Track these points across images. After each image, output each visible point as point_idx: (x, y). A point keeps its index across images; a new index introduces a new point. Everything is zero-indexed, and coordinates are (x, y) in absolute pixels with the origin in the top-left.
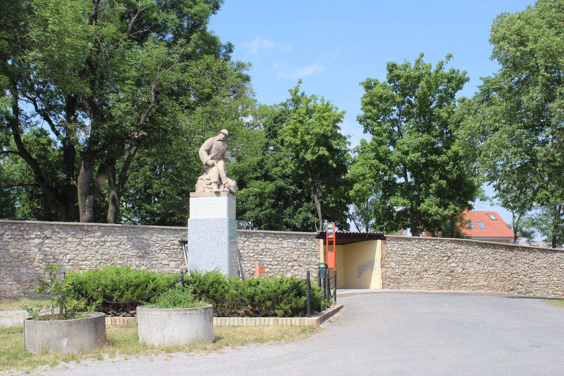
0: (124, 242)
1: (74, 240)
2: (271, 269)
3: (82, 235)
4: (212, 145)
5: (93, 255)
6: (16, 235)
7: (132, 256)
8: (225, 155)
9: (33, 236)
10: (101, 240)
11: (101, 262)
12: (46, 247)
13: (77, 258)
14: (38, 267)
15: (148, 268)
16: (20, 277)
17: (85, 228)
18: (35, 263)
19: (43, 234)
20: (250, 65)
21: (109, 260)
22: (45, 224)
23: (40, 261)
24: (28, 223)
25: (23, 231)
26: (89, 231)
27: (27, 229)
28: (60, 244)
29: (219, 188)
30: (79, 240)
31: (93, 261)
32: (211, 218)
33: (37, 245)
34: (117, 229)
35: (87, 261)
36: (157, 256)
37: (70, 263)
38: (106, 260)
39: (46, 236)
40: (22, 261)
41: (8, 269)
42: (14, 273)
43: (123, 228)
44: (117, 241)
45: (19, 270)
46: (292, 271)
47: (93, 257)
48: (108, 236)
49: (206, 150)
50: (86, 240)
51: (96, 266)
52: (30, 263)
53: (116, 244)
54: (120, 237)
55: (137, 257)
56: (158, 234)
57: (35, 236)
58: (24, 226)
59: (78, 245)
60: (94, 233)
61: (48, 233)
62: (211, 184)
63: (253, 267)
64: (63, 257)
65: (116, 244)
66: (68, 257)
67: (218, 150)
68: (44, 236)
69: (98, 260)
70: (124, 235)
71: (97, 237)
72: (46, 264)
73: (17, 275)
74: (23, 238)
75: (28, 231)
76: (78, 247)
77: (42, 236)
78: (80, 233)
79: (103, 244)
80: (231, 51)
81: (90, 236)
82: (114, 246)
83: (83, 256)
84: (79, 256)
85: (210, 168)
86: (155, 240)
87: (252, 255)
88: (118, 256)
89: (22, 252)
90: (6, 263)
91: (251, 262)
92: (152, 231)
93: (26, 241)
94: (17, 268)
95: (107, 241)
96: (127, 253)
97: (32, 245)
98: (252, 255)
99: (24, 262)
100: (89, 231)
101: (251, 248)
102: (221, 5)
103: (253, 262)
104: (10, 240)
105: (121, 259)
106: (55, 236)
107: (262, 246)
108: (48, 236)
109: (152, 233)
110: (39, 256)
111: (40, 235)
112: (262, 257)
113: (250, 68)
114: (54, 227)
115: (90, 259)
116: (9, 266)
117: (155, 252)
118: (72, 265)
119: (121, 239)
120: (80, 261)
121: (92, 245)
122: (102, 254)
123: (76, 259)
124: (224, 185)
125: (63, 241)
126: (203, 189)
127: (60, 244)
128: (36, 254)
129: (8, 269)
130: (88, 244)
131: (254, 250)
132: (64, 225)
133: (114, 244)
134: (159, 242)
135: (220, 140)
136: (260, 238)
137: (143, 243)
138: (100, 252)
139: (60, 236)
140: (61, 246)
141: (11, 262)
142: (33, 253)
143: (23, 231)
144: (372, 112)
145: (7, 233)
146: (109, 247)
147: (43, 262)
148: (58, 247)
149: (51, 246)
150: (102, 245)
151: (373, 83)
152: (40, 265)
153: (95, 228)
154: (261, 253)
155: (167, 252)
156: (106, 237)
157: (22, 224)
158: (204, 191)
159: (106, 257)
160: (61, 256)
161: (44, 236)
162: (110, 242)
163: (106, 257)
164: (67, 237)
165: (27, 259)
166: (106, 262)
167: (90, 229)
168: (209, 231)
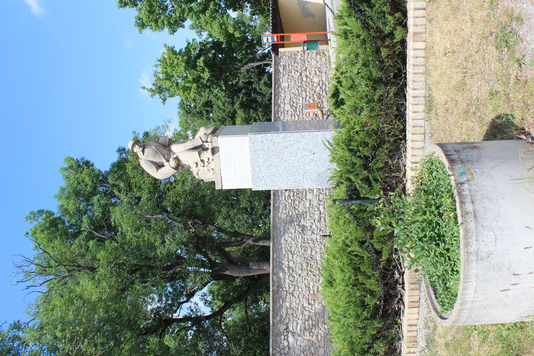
0: (289, 248)
1: (288, 299)
2: (310, 98)
3: (283, 292)
4: (150, 161)
5: (303, 279)
8: (164, 143)
10: (287, 271)
11: (310, 271)
12: (296, 328)
13: (307, 296)
14: (317, 336)
15: (315, 221)
17: (276, 288)
18: (313, 340)
19: (284, 333)
20: (134, 132)
21: (308, 262)
22: (273, 331)
23: (312, 334)
26: (279, 284)
27: (279, 350)
28: (293, 314)
29: (207, 149)
30: (288, 294)
31: (309, 279)
32: (249, 158)
33: (295, 338)
34: (275, 256)
35: (309, 285)
36: (301, 213)
37: (313, 303)
39: (285, 329)
40: (312, 354)
43: (275, 249)
44: (288, 255)
46: (311, 77)
47: (305, 279)
48: (283, 264)
49: (157, 170)
50: (288, 287)
51: (315, 275)
52: (314, 344)
54: (284, 252)
55: (303, 233)
56: (279, 212)
57: (285, 341)
58: (276, 354)
59: (293, 296)
60: (280, 279)
61: (282, 328)
62: (202, 161)
63: (309, 115)
64: (306, 310)
65: (291, 256)
66: (306, 305)
67: (156, 153)
68: (285, 332)
69: (308, 274)
70: (282, 247)
72: (314, 328)
77: (285, 334)
78: (281, 294)
79: (291, 269)
80: (124, 149)
81: (284, 282)
82: (293, 257)
83: (304, 290)
84: (305, 293)
85: (181, 163)
86: (285, 216)
87: (297, 117)
88: (303, 253)
89: (302, 354)
91: (304, 117)
92: (277, 219)
93: (292, 351)
95: (288, 265)
98: (297, 117)
99: (313, 351)
100: (279, 284)
101: (289, 118)
102: (86, 159)
103: (304, 115)
105: (306, 249)
106: (285, 320)
107: (287, 108)
108: (285, 328)
109: (278, 219)
110: (307, 336)
111: (285, 336)
112: (298, 107)
113: (137, 132)
114: (275, 322)
117: (297, 214)
118: (314, 300)
119: (286, 251)
120: (310, 293)
121: (293, 280)
122: (302, 269)
123: (308, 297)
124: (203, 142)
125: (290, 312)
126: (211, 171)
127: (293, 314)
128: (304, 339)
130: (292, 285)
131: (292, 115)
132: (273, 311)
133: (290, 258)
134: (287, 211)
135: (143, 151)
136: (280, 110)
138: (300, 272)
139: (284, 315)
140: (295, 313)
142: (303, 342)
143: (281, 354)
144: (164, 20)
146: (294, 263)
147: (312, 332)
148: (296, 316)
149: (295, 324)
150: (293, 271)
151: (138, 21)
152: (315, 334)
153: (275, 279)
154: (294, 107)
155: (297, 203)
156: (284, 266)
158: (213, 169)
159: (304, 265)
160: (305, 312)
161: (285, 332)
162: (289, 262)
163: (304, 265)
166: (309, 265)
167: (277, 284)
168: (269, 160)
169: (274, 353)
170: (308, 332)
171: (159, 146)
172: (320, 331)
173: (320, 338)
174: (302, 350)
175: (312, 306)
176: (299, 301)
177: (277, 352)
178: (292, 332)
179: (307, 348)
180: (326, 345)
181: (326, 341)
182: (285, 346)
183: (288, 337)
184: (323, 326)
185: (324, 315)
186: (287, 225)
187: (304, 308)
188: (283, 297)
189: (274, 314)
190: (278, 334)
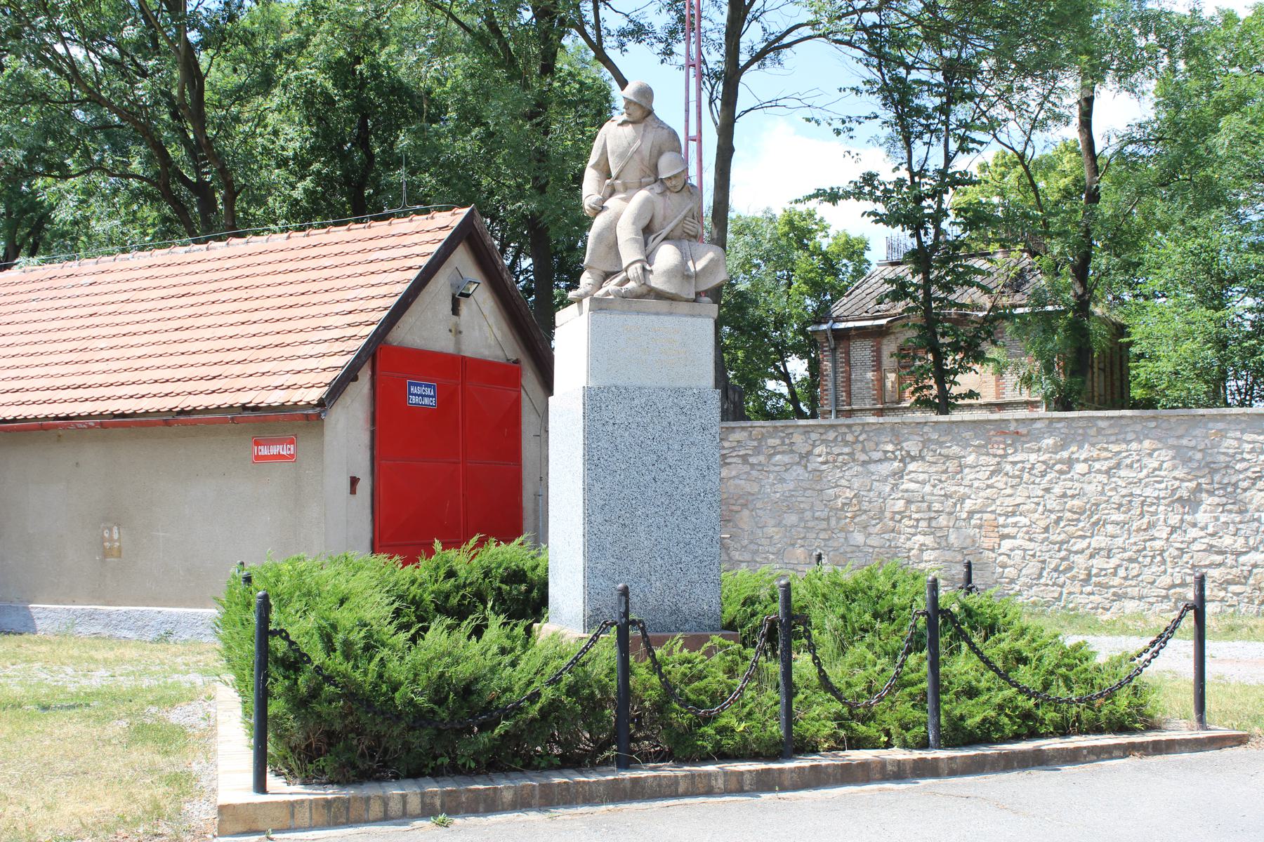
0: (1128, 461)
1: (983, 459)
3: (1002, 446)
5: (1036, 500)
7: (1158, 498)
10: (1058, 457)
11: (1059, 519)
12: (911, 480)
13: (993, 508)
14: (893, 531)
15: (1212, 535)
16: (849, 555)
17: (1012, 429)
19: (901, 449)
21: (1085, 512)
23: (898, 517)
24: (863, 425)
25: (854, 443)
26: (1022, 435)
27: (861, 438)
28: (945, 472)
30: (998, 459)
31: (1037, 515)
33: (887, 476)
34: (1102, 424)
35: (1021, 515)
36: (1239, 497)
37: (973, 522)
38: (1075, 513)
39: (908, 452)
41: (822, 535)
42: (835, 544)
43: (1123, 422)
44: (1106, 459)
45: (846, 539)
47: (1038, 504)
48: (1081, 447)
50: (1016, 459)
51: (1046, 529)
53: (1105, 465)
54: (1115, 448)
55: (1173, 502)
56: (1243, 431)
58: (852, 432)
59: (993, 473)
60: (1038, 439)
65: (1104, 468)
66: (968, 504)
69: (1051, 511)
70: (1131, 441)
71: (1047, 451)
72: (911, 523)
73: (842, 551)
74: (854, 460)
75: (865, 443)
76: (994, 479)
77: (898, 453)
79: (1065, 468)
81: (1029, 448)
82: (1099, 471)
83: (1008, 501)
84: (998, 503)
86: (1231, 451)
88: (1112, 500)
92: (1220, 425)
94: (843, 535)
95: (1077, 460)
96: (1138, 492)
97: (873, 477)
100: (1022, 435)
104: (824, 467)
105: (1122, 509)
106: (931, 453)
108: (912, 454)
109: (1221, 430)
111: (893, 452)
114: (926, 429)
115: (1028, 511)
116: (824, 530)
117: (1235, 485)
118: (980, 527)
119: (1120, 452)
120: (1000, 515)
121: (1033, 472)
122: (1064, 495)
123: (989, 510)
125: (952, 465)
127: (945, 472)
129: (822, 535)
130: (1023, 470)
133: (1097, 465)
137: (1190, 459)
138: (1057, 490)
139: (944, 451)
141: (828, 519)
145: (817, 451)
146: (1084, 475)
148: (940, 481)
149: (921, 477)
150: (1061, 472)
152: (898, 525)
153: (1038, 425)
156: (1074, 449)
157: (849, 426)
159: (1076, 503)
161: (903, 453)
162: (1085, 461)
163: (1076, 502)
164: (962, 453)
165: (865, 511)
166: (1076, 516)
167: (1023, 430)
170: (902, 509)
171: (642, 160)
172: (903, 537)
173: (886, 536)
175: (964, 520)
176: (978, 488)
177: (856, 434)
178: (904, 470)
179: (865, 506)
180: (871, 550)
181: (882, 550)
182: (870, 454)
184: (917, 546)
185: (943, 548)
186: (1199, 456)
187: (962, 500)
188: (990, 446)
189: (946, 425)
190: (898, 436)
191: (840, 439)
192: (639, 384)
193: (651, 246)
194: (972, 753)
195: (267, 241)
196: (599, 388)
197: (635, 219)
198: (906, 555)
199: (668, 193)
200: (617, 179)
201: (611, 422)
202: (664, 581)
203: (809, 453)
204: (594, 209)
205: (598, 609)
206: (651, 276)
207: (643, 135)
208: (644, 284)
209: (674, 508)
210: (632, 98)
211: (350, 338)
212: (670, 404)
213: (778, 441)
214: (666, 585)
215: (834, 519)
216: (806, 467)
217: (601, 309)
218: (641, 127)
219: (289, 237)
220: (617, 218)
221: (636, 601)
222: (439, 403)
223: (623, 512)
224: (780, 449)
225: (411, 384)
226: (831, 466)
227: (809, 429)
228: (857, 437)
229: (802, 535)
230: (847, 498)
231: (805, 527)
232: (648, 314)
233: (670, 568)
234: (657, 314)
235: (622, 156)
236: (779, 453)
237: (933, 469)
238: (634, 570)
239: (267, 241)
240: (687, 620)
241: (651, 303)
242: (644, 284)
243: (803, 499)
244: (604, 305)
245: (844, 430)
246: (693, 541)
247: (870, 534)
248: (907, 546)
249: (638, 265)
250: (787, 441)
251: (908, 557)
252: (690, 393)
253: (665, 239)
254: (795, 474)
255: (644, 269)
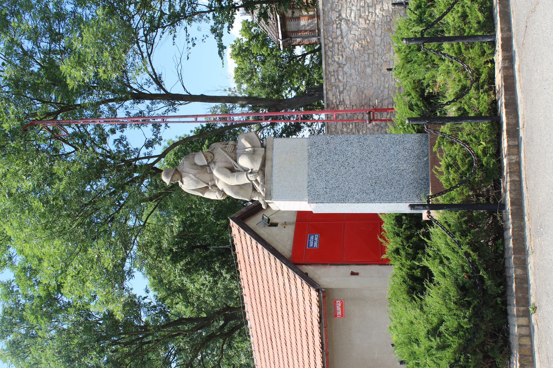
6: (338, 50)
9: (339, 32)
12: (350, 16)
14: (374, 24)
16: (386, 44)
23: (367, 22)
25: (333, 43)
27: (331, 40)
33: (348, 27)
39: (337, 18)
41: (376, 56)
42: (380, 50)
45: (378, 46)
52: (370, 33)
58: (328, 44)
61: (334, 16)
68: (337, 20)
72: (370, 15)
73: (383, 48)
74: (341, 43)
77: (337, 22)
90: (370, 59)
93: (345, 40)
94: (376, 47)
99: (368, 40)
106: (337, 7)
108: (338, 16)
110: (362, 24)
111: (337, 25)
114: (326, 10)
116: (374, 56)
128: (359, 28)
141: (369, 54)
145: (337, 59)
147: (368, 19)
148: (350, 2)
149: (348, 11)
152: (371, 22)
157: (325, 45)
161: (337, 20)
165: (365, 37)
169: (326, 43)
170: (364, 20)
171: (199, 173)
172: (377, 19)
173: (376, 26)
174: (356, 39)
177: (329, 42)
178: (345, 19)
179: (362, 37)
180: (383, 34)
181: (383, 29)
182: (338, 35)
183: (341, 25)
184: (381, 12)
190: (329, 23)
191: (331, 49)
192: (306, 175)
193: (240, 169)
194: (498, 18)
195: (247, 304)
196: (309, 195)
197: (227, 177)
198: (385, 17)
199: (214, 160)
200: (208, 184)
201: (325, 189)
202: (403, 163)
203: (338, 63)
204: (223, 196)
205: (417, 196)
206: (254, 170)
207: (187, 173)
208: (258, 173)
209: (367, 158)
210: (169, 179)
211: (288, 276)
212: (316, 160)
213: (333, 78)
214: (405, 162)
215: (368, 51)
216: (344, 65)
217: (270, 194)
218: (183, 174)
219: (245, 295)
220: (227, 185)
221: (413, 177)
222: (317, 233)
223: (369, 183)
224: (336, 77)
225: (309, 247)
226: (344, 54)
227: (327, 64)
228: (330, 41)
229: (376, 66)
230: (359, 46)
231: (372, 65)
232: (272, 171)
233: (397, 159)
234: (272, 166)
235: (197, 183)
236: (338, 77)
237: (345, 6)
238: (397, 178)
239: (247, 304)
240: (423, 151)
241: (267, 169)
242: (258, 173)
243: (359, 65)
244: (268, 193)
245: (327, 47)
246: (383, 148)
247: (376, 34)
248: (381, 17)
249: (249, 176)
250: (333, 73)
251: (386, 16)
252: (310, 150)
253: (236, 161)
254: (348, 70)
255: (251, 173)
